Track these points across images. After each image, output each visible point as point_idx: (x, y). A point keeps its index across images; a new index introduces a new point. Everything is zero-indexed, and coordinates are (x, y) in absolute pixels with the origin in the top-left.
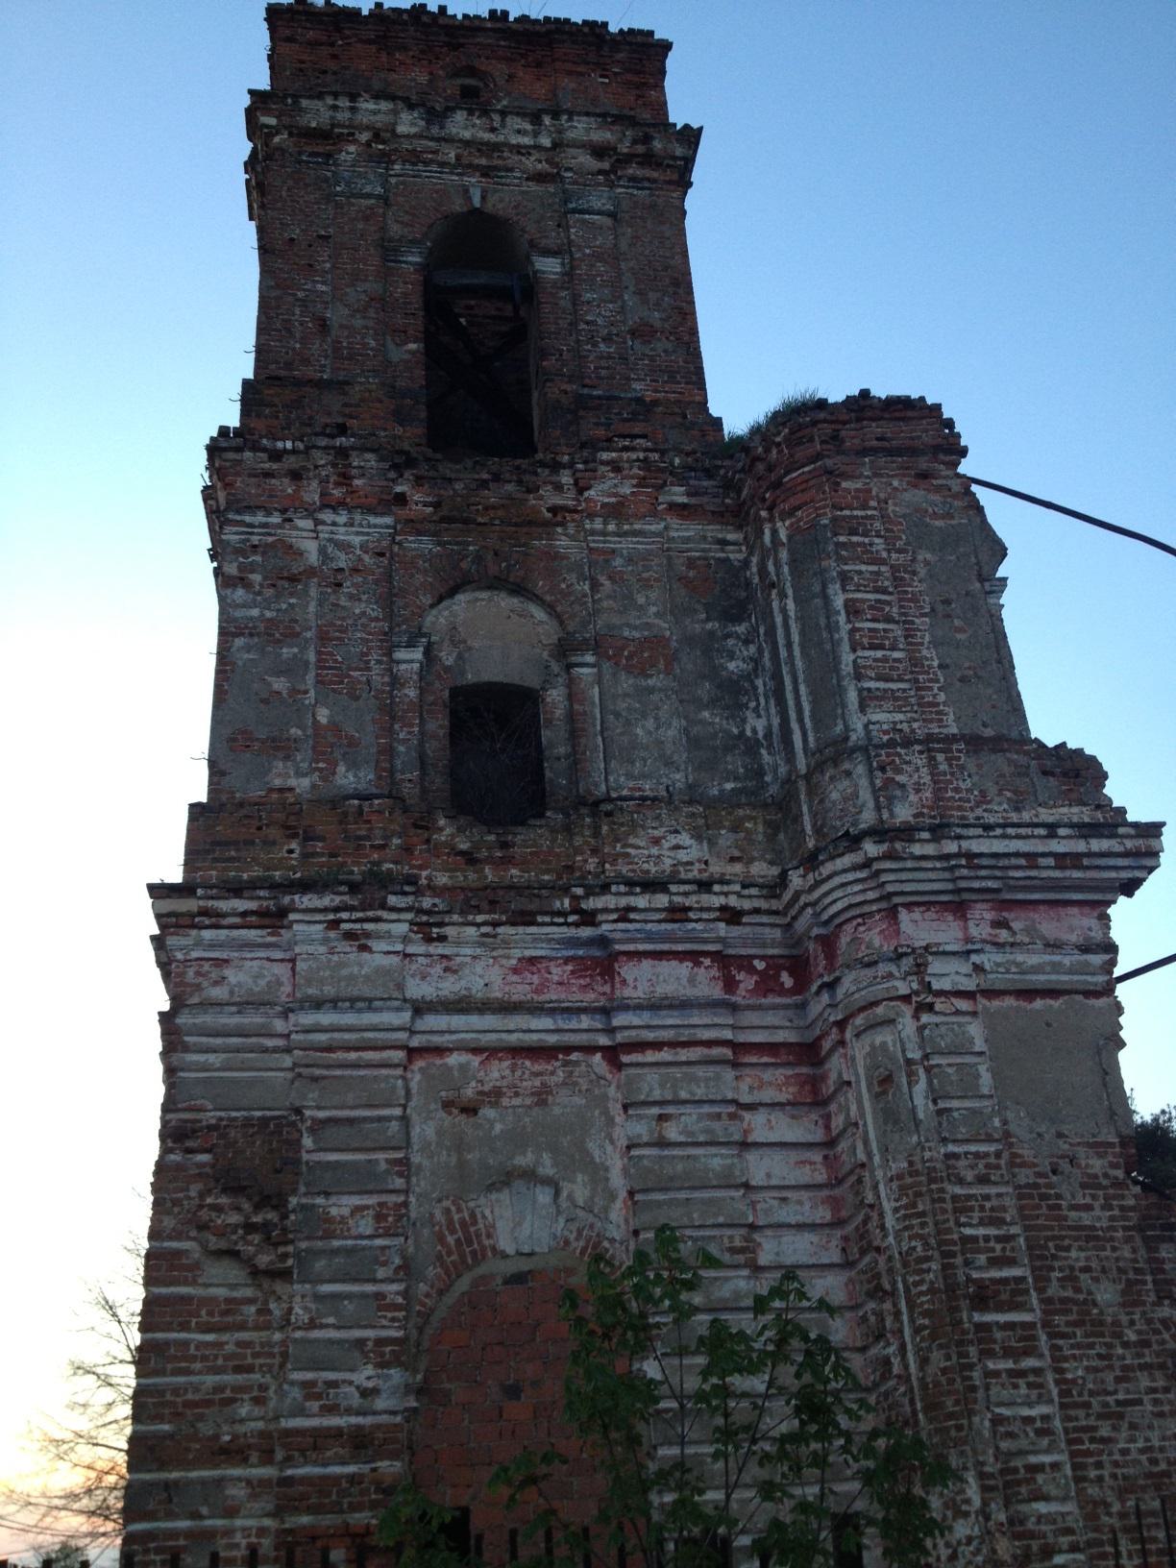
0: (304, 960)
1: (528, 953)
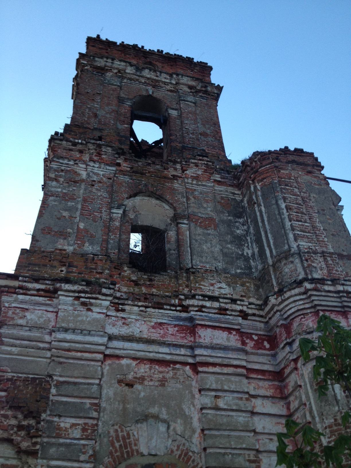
0: (61, 312)
1: (159, 321)
